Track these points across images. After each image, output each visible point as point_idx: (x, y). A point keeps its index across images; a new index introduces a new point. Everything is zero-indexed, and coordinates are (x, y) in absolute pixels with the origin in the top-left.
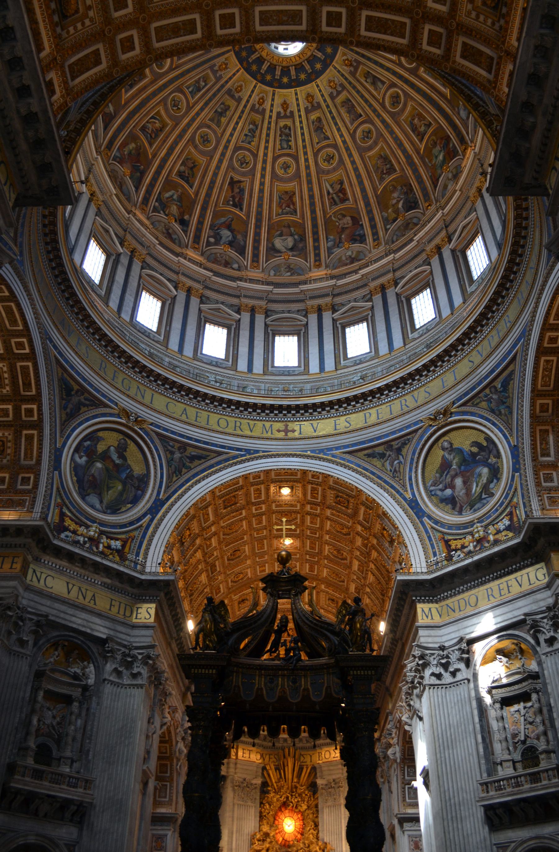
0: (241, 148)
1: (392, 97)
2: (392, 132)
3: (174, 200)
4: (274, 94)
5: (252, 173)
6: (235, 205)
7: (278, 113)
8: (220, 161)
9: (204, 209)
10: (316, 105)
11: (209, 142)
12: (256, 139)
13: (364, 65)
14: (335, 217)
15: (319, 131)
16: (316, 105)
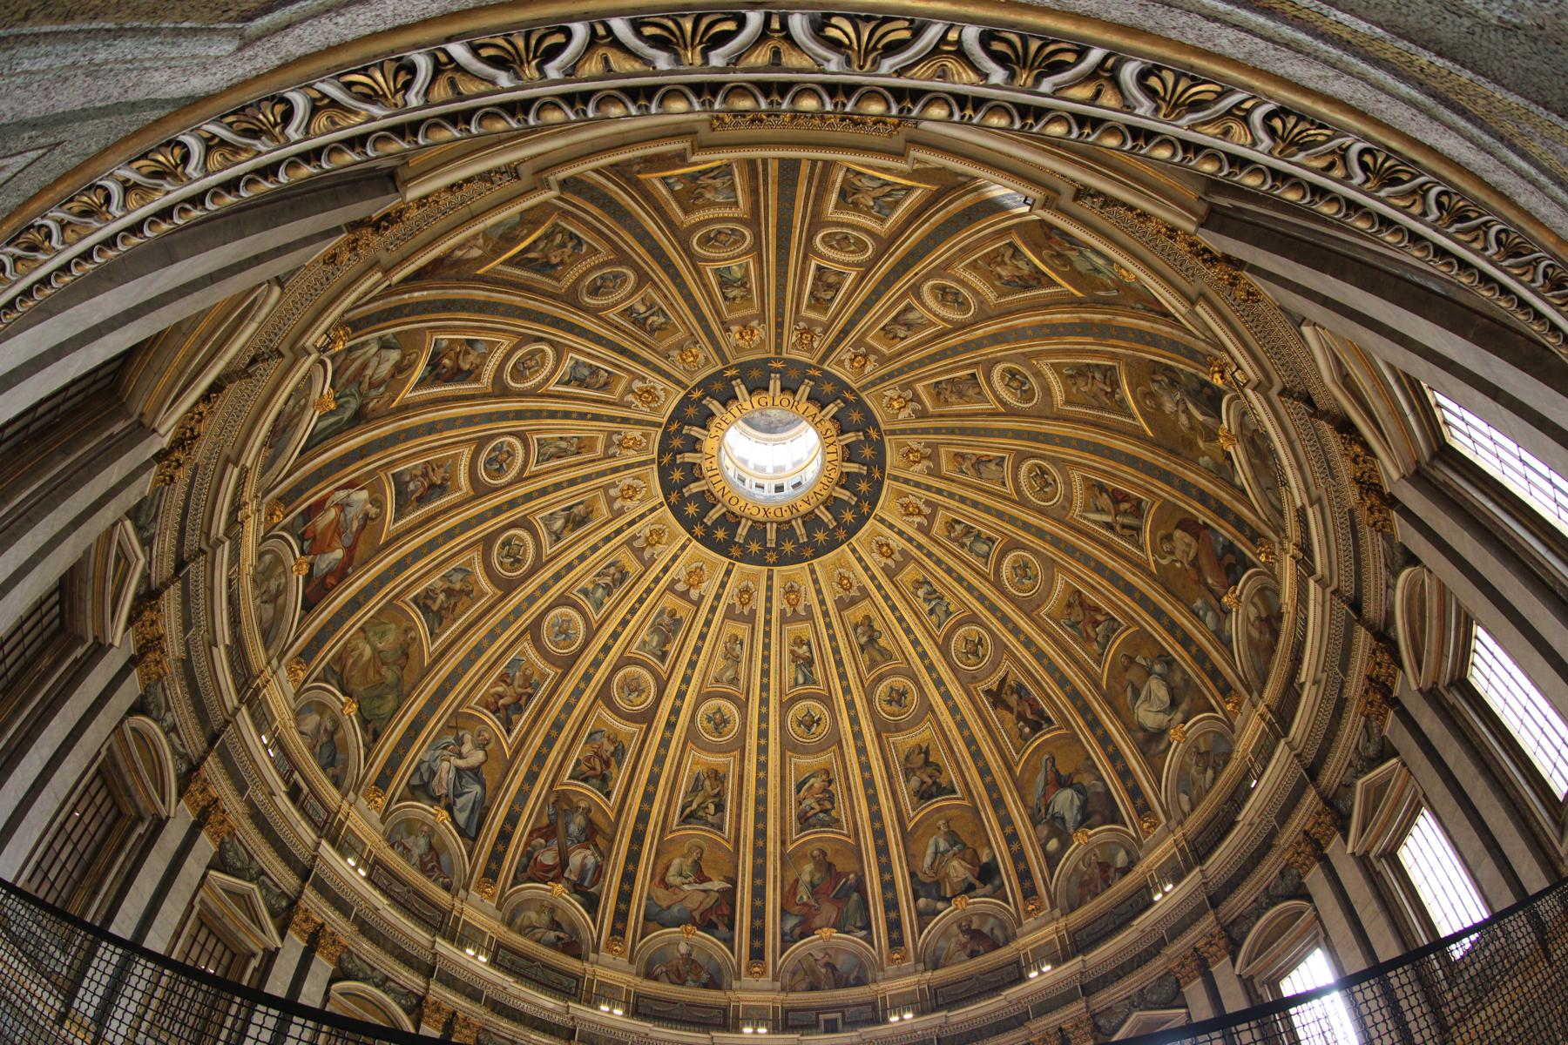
0: (948, 638)
1: (943, 302)
2: (1018, 334)
3: (943, 853)
4: (882, 521)
5: (1000, 646)
6: (1036, 728)
7: (920, 528)
8: (946, 696)
9: (998, 804)
10: (929, 451)
11: (903, 694)
12: (948, 597)
13: (865, 334)
14: (1164, 558)
15: (982, 469)
16: (929, 451)
